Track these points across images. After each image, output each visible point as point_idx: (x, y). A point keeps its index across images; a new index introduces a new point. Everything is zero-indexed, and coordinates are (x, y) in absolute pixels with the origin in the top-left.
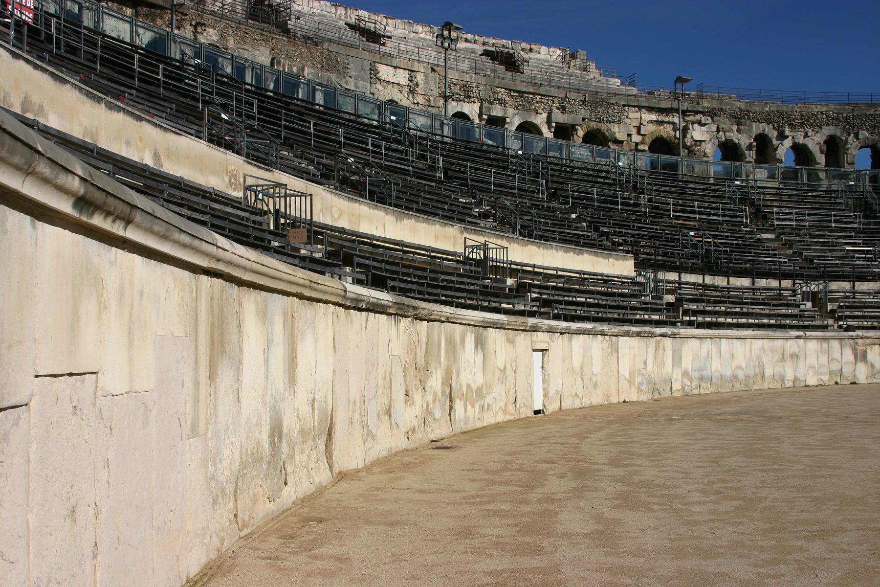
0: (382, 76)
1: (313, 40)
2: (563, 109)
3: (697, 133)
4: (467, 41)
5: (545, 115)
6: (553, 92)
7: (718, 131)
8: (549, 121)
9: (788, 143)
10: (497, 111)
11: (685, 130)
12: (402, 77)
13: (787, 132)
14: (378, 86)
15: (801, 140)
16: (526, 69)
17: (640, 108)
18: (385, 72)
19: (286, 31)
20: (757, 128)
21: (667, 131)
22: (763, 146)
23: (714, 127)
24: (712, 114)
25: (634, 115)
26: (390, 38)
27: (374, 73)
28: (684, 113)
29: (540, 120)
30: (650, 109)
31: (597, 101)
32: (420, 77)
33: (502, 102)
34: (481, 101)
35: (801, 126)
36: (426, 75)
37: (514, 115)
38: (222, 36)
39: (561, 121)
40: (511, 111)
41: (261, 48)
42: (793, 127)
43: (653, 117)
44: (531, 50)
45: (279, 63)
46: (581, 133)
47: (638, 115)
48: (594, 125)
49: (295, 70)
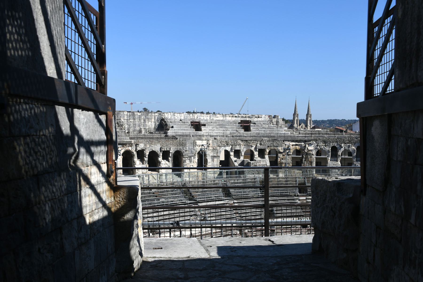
0: (197, 144)
1: (174, 138)
2: (261, 144)
3: (310, 148)
4: (236, 117)
5: (254, 146)
6: (258, 138)
7: (317, 146)
8: (256, 149)
9: (342, 149)
10: (238, 148)
11: (305, 146)
12: (204, 143)
13: (343, 145)
14: (197, 147)
15: (347, 148)
16: (252, 128)
17: (289, 141)
18: (199, 142)
19: (166, 136)
20: (331, 145)
21: (298, 148)
22: (334, 150)
23: (316, 144)
24: (316, 140)
25: (287, 143)
26: (204, 125)
27: (194, 144)
28: (305, 141)
29: (253, 149)
30: (293, 141)
31: (274, 139)
32: (211, 142)
33: (240, 145)
34: (232, 145)
35: (348, 143)
36: (213, 141)
37: (244, 148)
38: (145, 145)
39: (259, 148)
40: (242, 147)
41: (158, 145)
42: (345, 143)
43: (294, 143)
44: (259, 117)
45: (163, 148)
46: (268, 151)
47: (288, 143)
48: (273, 148)
49: (168, 149)
